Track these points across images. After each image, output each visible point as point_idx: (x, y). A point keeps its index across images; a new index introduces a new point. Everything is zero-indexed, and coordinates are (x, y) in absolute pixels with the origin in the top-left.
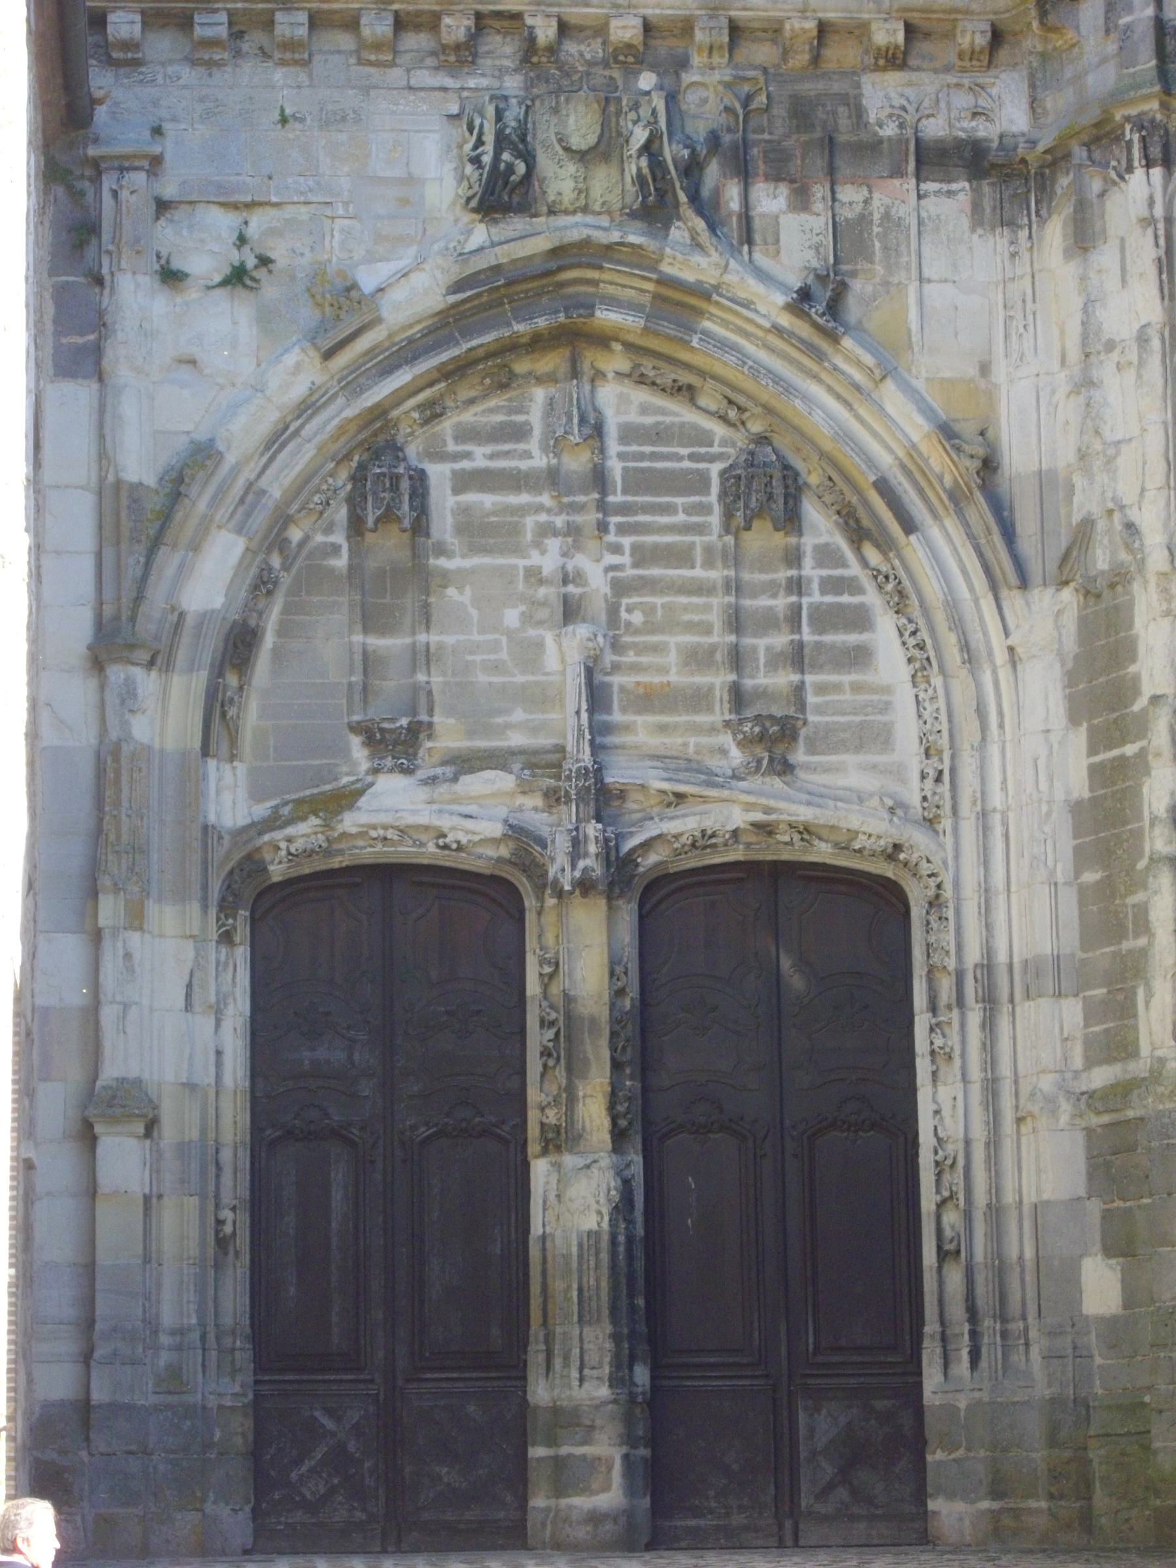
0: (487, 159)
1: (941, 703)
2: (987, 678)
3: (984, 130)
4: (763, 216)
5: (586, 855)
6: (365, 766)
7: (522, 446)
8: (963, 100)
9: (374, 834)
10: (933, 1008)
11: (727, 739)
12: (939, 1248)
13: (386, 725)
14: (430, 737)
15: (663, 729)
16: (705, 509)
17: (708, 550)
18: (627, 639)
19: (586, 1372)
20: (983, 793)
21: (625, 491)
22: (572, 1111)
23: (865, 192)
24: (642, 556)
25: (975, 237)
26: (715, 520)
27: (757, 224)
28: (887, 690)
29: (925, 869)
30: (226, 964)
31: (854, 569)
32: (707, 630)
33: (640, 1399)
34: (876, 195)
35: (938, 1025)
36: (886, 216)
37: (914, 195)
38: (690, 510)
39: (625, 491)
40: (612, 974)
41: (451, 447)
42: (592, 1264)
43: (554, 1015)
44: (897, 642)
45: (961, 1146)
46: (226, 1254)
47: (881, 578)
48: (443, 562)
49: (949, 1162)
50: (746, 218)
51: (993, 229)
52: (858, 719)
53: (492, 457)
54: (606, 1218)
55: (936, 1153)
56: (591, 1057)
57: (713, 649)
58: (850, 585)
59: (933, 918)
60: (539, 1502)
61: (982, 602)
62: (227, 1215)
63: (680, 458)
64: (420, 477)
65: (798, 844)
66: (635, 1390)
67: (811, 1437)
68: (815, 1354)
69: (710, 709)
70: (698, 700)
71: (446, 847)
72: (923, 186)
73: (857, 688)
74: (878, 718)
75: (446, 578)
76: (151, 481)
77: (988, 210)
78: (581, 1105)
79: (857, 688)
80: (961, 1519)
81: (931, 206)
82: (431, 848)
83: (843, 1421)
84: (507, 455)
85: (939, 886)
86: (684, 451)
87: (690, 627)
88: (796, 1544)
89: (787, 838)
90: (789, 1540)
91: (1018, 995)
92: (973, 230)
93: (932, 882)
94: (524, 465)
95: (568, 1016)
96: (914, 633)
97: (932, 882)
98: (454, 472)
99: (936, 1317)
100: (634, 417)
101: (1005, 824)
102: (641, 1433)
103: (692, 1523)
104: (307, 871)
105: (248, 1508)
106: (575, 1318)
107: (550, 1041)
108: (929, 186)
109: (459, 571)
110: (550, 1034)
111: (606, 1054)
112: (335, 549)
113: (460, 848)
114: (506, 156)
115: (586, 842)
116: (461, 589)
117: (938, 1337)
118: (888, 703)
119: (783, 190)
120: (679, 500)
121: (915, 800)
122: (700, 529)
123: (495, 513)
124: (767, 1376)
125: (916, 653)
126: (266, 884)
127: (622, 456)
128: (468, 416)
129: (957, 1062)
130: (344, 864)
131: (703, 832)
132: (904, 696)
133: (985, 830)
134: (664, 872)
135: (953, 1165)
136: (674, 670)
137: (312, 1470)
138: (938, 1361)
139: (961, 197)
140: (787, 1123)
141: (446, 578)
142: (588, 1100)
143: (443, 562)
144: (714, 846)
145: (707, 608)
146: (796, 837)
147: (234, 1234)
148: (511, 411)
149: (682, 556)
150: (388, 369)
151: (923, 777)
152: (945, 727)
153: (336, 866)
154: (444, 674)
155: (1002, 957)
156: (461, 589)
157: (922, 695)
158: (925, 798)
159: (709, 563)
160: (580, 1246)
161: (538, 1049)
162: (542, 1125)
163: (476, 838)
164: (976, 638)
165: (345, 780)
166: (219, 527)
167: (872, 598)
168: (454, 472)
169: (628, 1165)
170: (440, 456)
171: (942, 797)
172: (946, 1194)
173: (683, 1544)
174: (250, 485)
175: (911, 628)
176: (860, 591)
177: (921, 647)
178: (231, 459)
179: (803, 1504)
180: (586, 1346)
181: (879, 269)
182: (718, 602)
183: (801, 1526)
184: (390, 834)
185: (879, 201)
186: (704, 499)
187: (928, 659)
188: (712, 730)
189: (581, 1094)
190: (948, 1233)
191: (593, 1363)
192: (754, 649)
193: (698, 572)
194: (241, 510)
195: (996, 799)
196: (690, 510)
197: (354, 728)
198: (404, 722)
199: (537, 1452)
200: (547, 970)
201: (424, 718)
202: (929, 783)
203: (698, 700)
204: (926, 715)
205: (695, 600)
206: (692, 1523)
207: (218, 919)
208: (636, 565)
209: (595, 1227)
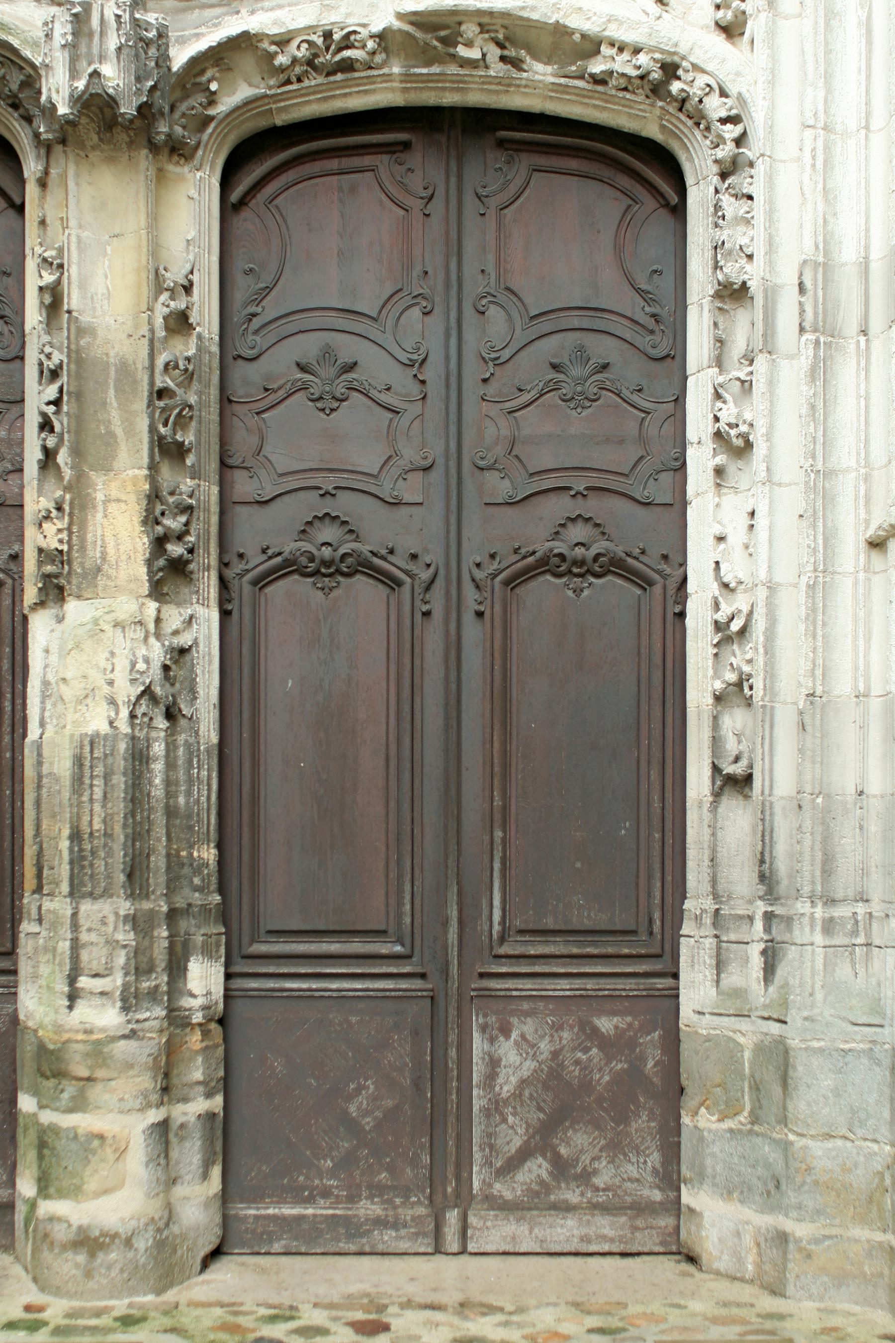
5: (102, 58)
10: (719, 362)
12: (716, 769)
19: (84, 982)
22: (83, 526)
29: (715, 107)
33: (198, 1018)
40: (158, 285)
42: (98, 793)
43: (57, 357)
45: (762, 593)
49: (735, 626)
55: (717, 607)
56: (119, 432)
59: (726, 200)
65: (497, 69)
66: (187, 1002)
67: (491, 1077)
68: (502, 939)
78: (99, 515)
83: (545, 1047)
85: (739, 141)
89: (474, 54)
90: (452, 1242)
91: (876, 324)
95: (77, 356)
97: (730, 132)
99: (706, 887)
103: (289, 1211)
106: (65, 888)
107: (49, 403)
110: (51, 392)
111: (143, 424)
115: (102, 34)
117: (708, 920)
124: (423, 976)
129: (760, 449)
134: (263, 123)
140: (471, 557)
142: (113, 508)
144: (348, 66)
146: (494, 52)
160: (78, 761)
162: (41, 550)
169: (190, 620)
173: (277, 1247)
179: (476, 1184)
180: (84, 937)
183: (472, 1220)
189: (100, 496)
190: (731, 746)
191: (95, 967)
206: (289, 1211)
209: (104, 728)
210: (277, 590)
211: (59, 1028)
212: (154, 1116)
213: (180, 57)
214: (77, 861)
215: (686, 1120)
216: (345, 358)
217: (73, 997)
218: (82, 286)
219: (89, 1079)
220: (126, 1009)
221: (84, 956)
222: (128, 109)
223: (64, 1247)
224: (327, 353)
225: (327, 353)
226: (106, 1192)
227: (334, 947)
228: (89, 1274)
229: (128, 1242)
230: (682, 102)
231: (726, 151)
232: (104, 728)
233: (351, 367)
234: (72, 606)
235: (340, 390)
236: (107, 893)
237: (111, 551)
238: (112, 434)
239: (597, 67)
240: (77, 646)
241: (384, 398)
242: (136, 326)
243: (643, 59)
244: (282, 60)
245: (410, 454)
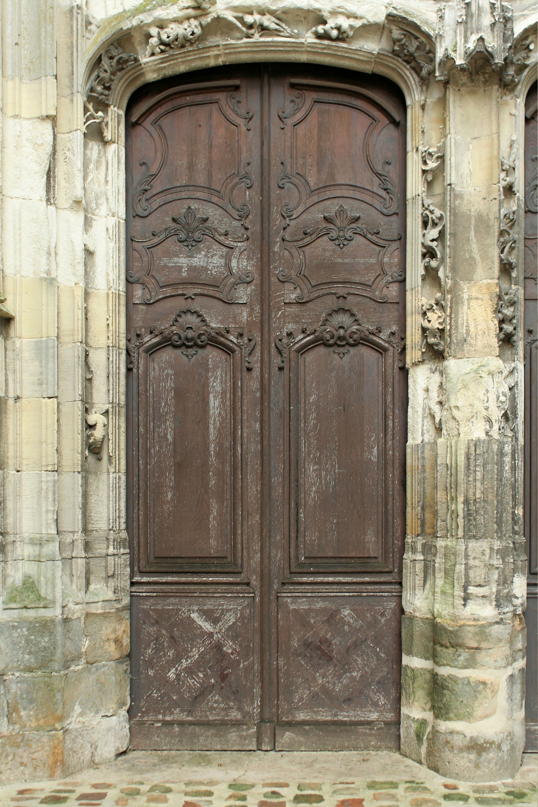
9: (249, 19)
19: (472, 590)
22: (457, 315)
30: (98, 162)
42: (479, 475)
46: (100, 460)
56: (477, 257)
62: (95, 418)
71: (325, 36)
78: (465, 307)
82: (309, 38)
104: (183, 68)
107: (433, 240)
110: (434, 233)
113: (342, 36)
115: (479, 15)
126: (139, 83)
130: (220, 61)
142: (473, 303)
147: (106, 437)
153: (212, 63)
161: (420, 250)
162: (424, 330)
163: (358, 23)
184: (268, 21)
189: (466, 296)
191: (478, 580)
207: (86, 110)
211: (455, 618)
213: (518, 28)
214: (468, 515)
217: (466, 599)
218: (457, 170)
219: (477, 648)
220: (498, 606)
221: (472, 574)
222: (499, 60)
223: (461, 750)
224: (341, 211)
225: (341, 211)
226: (486, 716)
228: (477, 766)
229: (499, 747)
232: (483, 436)
234: (451, 364)
235: (348, 234)
236: (484, 536)
237: (472, 329)
238: (472, 258)
240: (465, 387)
242: (489, 193)
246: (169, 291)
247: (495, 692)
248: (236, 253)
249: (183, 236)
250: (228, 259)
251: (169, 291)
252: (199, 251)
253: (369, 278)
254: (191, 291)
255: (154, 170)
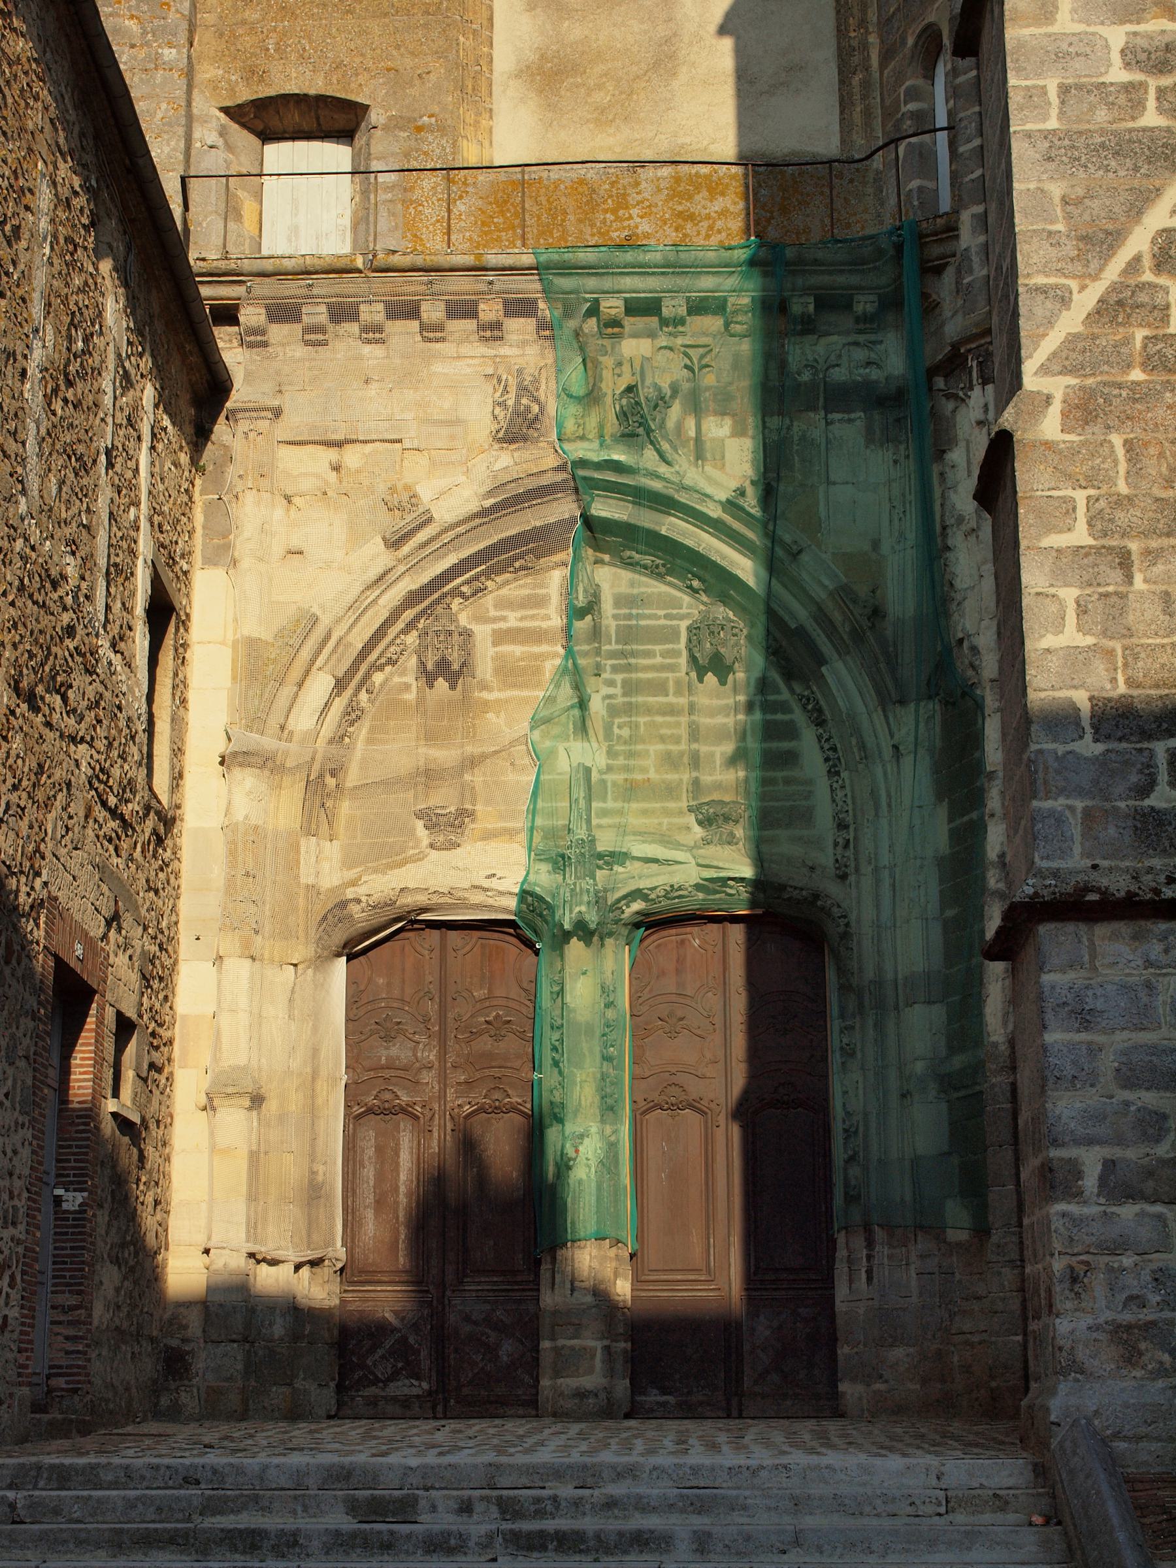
0: (510, 403)
1: (848, 790)
2: (879, 771)
3: (874, 374)
4: (713, 439)
6: (425, 842)
7: (543, 612)
8: (860, 354)
10: (842, 1016)
11: (691, 819)
12: (846, 1193)
13: (439, 811)
14: (473, 821)
15: (645, 812)
16: (675, 654)
17: (678, 683)
18: (618, 748)
20: (876, 854)
21: (617, 642)
23: (788, 421)
24: (630, 688)
25: (868, 451)
26: (683, 660)
27: (708, 445)
28: (810, 782)
31: (785, 695)
32: (677, 740)
34: (795, 423)
35: (846, 1028)
36: (803, 438)
37: (823, 422)
38: (666, 654)
39: (617, 642)
41: (493, 613)
44: (817, 746)
47: (804, 701)
48: (485, 695)
49: (853, 1129)
50: (698, 440)
51: (882, 445)
52: (788, 804)
53: (521, 619)
54: (593, 1170)
57: (681, 754)
58: (783, 707)
60: (545, 1382)
61: (875, 716)
63: (658, 618)
64: (467, 634)
69: (678, 799)
70: (670, 791)
72: (830, 416)
73: (788, 781)
74: (804, 803)
75: (486, 706)
76: (266, 635)
77: (878, 432)
79: (788, 781)
80: (860, 1399)
81: (836, 429)
84: (533, 617)
86: (661, 613)
87: (662, 739)
88: (740, 1417)
89: (733, 891)
90: (735, 1413)
91: (901, 1004)
92: (867, 447)
93: (842, 922)
94: (544, 625)
96: (827, 740)
97: (842, 922)
98: (494, 631)
100: (624, 589)
101: (892, 876)
102: (621, 1331)
105: (332, 1384)
108: (837, 416)
109: (498, 701)
110: (556, 1036)
111: (597, 1049)
112: (407, 687)
114: (524, 401)
116: (498, 714)
118: (810, 792)
119: (728, 422)
120: (658, 648)
121: (830, 862)
122: (672, 668)
123: (522, 659)
125: (830, 753)
127: (615, 617)
128: (504, 591)
129: (859, 1055)
131: (672, 886)
132: (822, 786)
133: (878, 882)
135: (856, 1132)
136: (652, 770)
137: (383, 1357)
138: (845, 1277)
139: (858, 423)
141: (486, 706)
143: (485, 695)
145: (678, 724)
148: (535, 586)
149: (660, 688)
150: (439, 553)
151: (836, 844)
152: (850, 808)
154: (484, 774)
155: (890, 976)
156: (498, 714)
157: (835, 785)
158: (837, 861)
159: (678, 693)
161: (549, 1046)
162: (552, 1103)
164: (870, 742)
165: (411, 852)
166: (320, 669)
167: (798, 716)
168: (494, 631)
170: (482, 619)
171: (849, 859)
172: (850, 1153)
173: (658, 1414)
174: (341, 639)
175: (826, 736)
176: (791, 711)
177: (834, 749)
178: (325, 621)
181: (798, 476)
182: (684, 720)
185: (797, 427)
186: (675, 646)
187: (839, 759)
188: (680, 813)
192: (712, 754)
193: (671, 699)
194: (335, 657)
195: (885, 859)
196: (666, 654)
197: (419, 815)
198: (452, 809)
199: (545, 1344)
200: (556, 989)
201: (468, 806)
202: (839, 849)
203: (670, 791)
204: (838, 799)
205: (668, 719)
208: (625, 695)
210: (651, 1117)
212: (606, 1342)
215: (839, 1352)
216: (680, 1014)
227: (679, 1277)
229: (596, 1395)
230: (822, 909)
231: (841, 929)
233: (682, 1019)
237: (583, 1103)
239: (786, 896)
241: (698, 1032)
243: (804, 893)
244: (653, 896)
245: (709, 1055)
246: (372, 1074)
247: (593, 1356)
248: (421, 1046)
249: (382, 1034)
250: (415, 1050)
251: (372, 1074)
252: (394, 1045)
253: (517, 1064)
254: (387, 1073)
255: (362, 988)
